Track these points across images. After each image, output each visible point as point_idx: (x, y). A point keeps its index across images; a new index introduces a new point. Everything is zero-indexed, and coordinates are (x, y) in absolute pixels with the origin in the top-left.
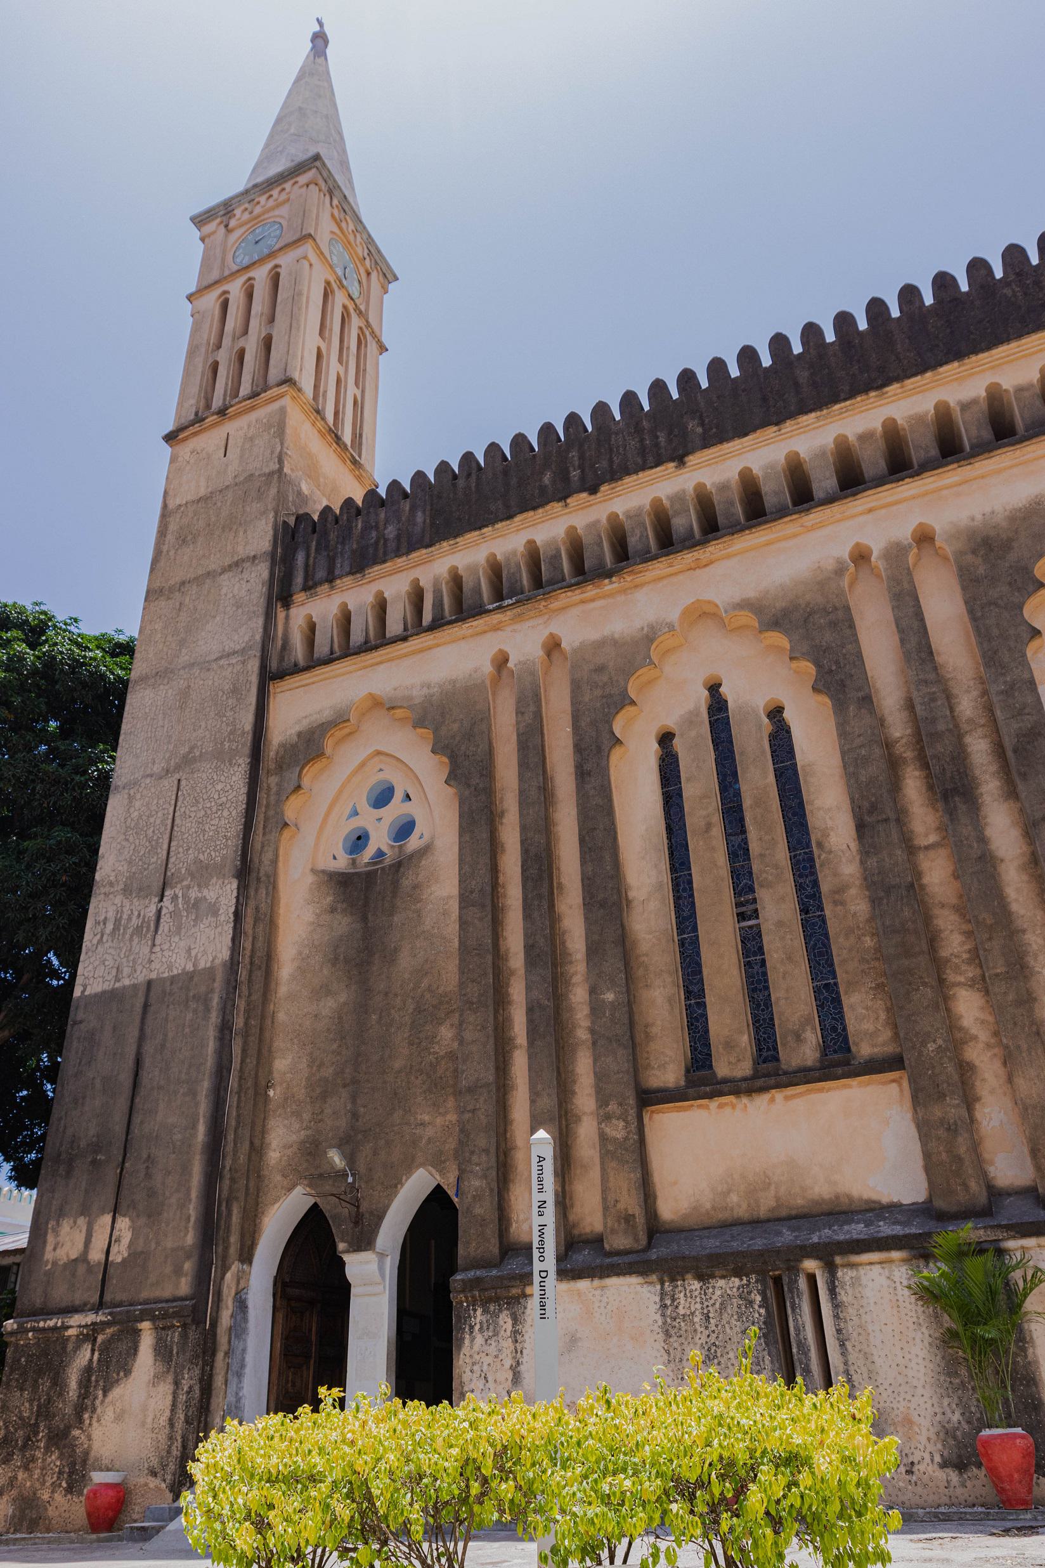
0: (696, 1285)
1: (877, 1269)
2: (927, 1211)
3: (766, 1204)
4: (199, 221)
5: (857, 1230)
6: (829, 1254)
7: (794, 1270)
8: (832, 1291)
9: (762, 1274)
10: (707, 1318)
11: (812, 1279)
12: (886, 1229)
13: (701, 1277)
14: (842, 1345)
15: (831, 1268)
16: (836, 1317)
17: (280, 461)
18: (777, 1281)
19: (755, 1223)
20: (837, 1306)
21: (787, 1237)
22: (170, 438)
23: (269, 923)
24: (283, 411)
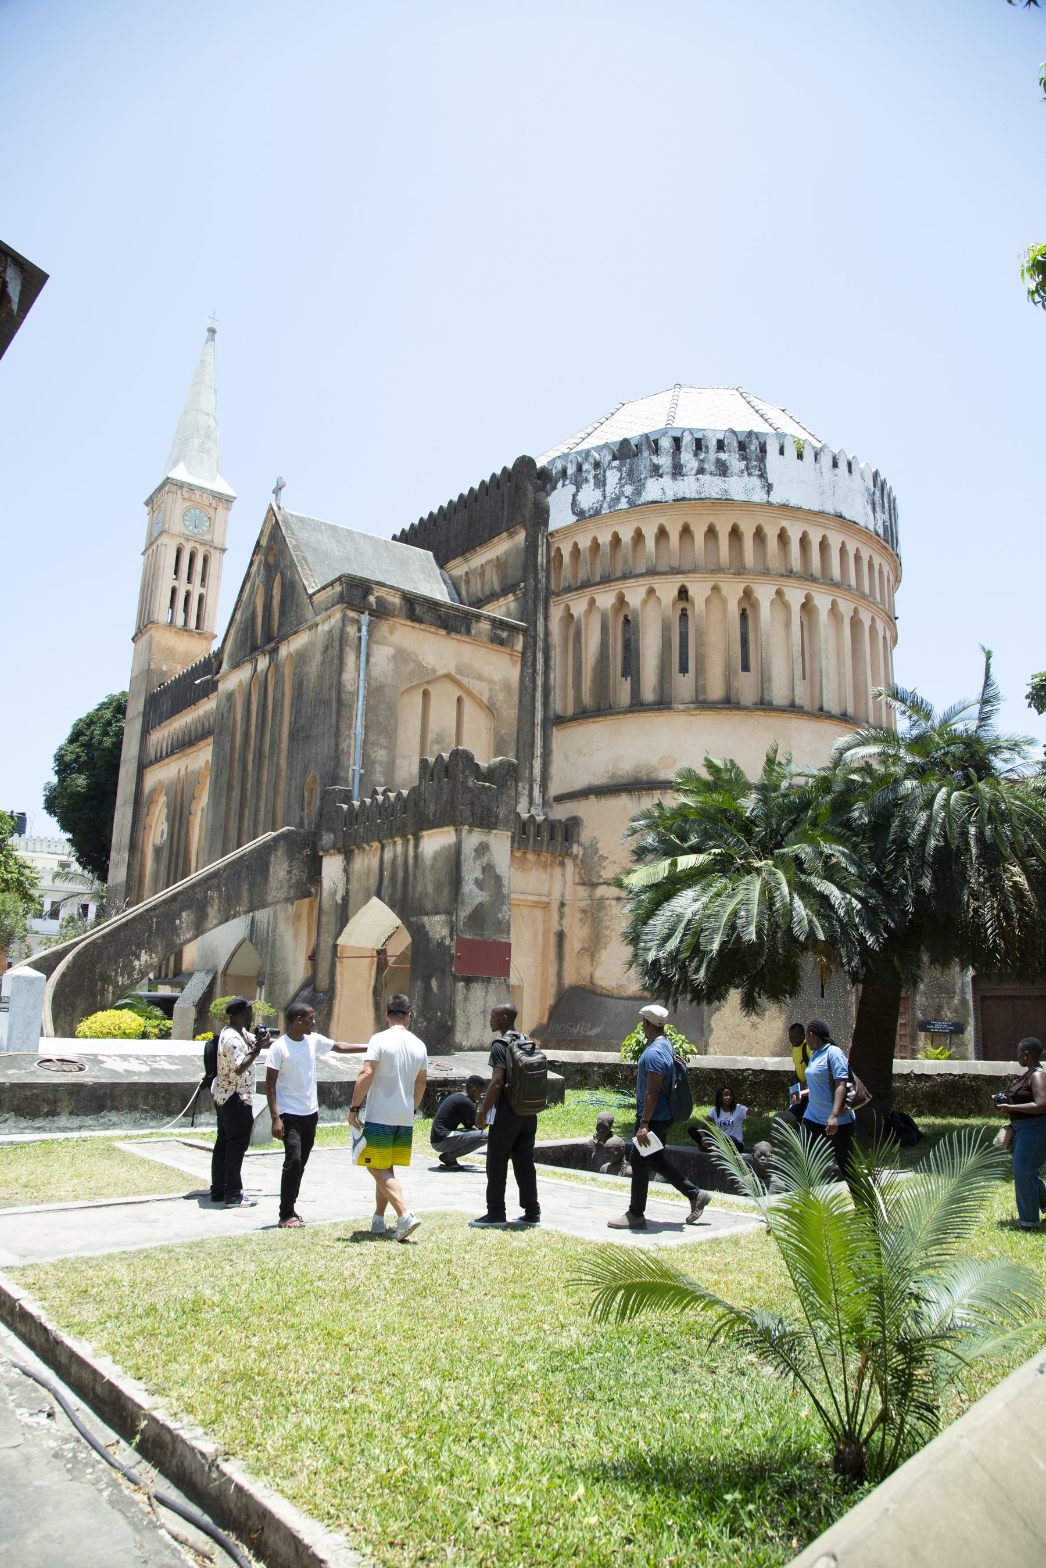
4: (147, 503)
17: (149, 665)
22: (133, 639)
23: (142, 865)
24: (151, 637)
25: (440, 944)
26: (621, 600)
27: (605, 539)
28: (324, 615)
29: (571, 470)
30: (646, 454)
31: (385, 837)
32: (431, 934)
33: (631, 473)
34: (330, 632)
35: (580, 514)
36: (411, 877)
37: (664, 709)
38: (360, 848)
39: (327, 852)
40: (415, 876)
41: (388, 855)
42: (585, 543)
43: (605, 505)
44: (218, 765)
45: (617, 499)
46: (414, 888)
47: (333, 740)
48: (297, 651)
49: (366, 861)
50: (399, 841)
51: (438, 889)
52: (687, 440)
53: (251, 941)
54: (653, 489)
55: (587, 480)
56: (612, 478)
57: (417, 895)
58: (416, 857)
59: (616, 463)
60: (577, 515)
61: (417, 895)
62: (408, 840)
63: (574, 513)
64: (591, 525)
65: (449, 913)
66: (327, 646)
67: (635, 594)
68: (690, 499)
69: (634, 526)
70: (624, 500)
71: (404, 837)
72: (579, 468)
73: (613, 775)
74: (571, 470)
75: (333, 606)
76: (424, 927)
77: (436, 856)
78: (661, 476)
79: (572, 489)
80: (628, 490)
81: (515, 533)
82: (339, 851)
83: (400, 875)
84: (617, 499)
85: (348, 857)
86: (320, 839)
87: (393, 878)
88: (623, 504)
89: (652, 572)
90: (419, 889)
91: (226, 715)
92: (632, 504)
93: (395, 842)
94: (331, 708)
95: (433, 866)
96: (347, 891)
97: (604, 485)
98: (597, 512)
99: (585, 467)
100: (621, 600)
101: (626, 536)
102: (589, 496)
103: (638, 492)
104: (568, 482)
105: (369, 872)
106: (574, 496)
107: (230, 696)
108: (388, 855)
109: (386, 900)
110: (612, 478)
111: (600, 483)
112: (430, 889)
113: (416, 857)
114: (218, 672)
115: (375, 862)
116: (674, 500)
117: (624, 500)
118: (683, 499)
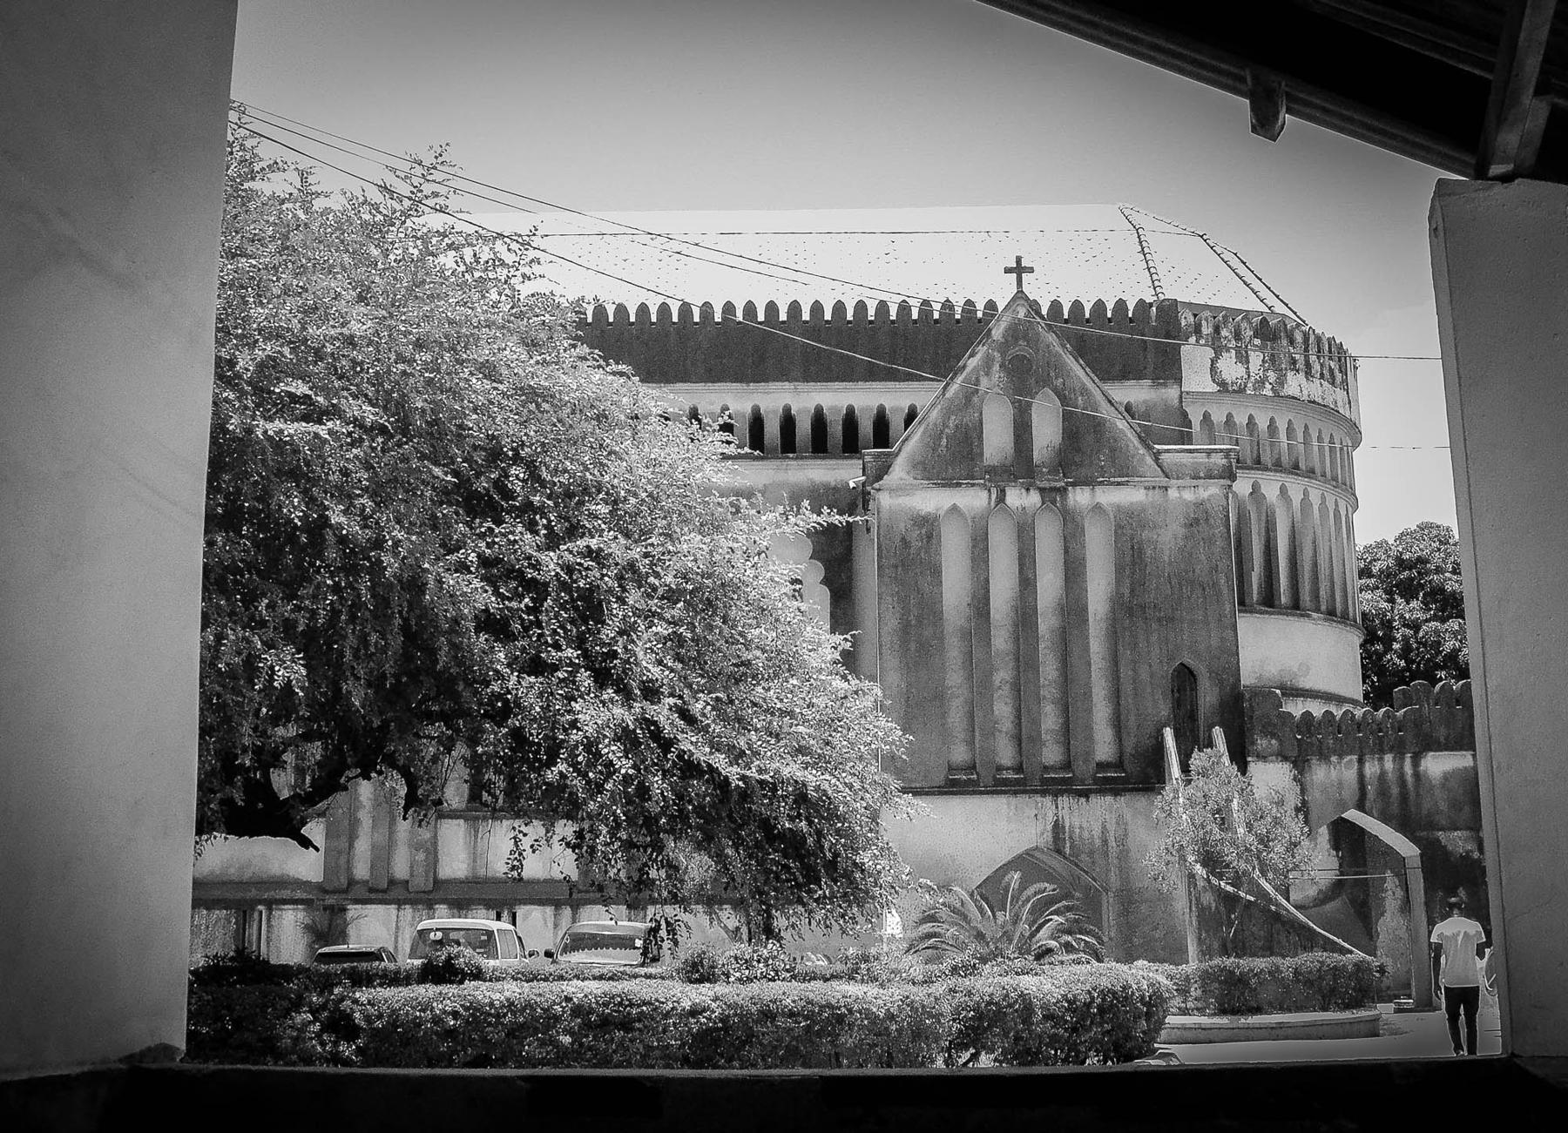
0: (205, 912)
1: (291, 912)
2: (321, 888)
3: (247, 875)
5: (286, 894)
6: (271, 904)
7: (253, 909)
8: (269, 920)
9: (238, 909)
10: (208, 927)
11: (261, 912)
12: (299, 895)
13: (207, 909)
14: (268, 943)
15: (270, 910)
16: (268, 931)
18: (245, 912)
19: (241, 884)
20: (269, 926)
21: (253, 893)
25: (1466, 857)
26: (1256, 488)
27: (1241, 419)
28: (1188, 482)
29: (1207, 330)
30: (1285, 342)
31: (1372, 753)
32: (1450, 848)
33: (1273, 358)
34: (1199, 504)
35: (1223, 384)
36: (1412, 795)
37: (1302, 616)
38: (1324, 757)
39: (1262, 757)
40: (1418, 795)
41: (1371, 769)
42: (1218, 417)
43: (1250, 385)
44: (906, 611)
45: (1261, 382)
46: (1419, 806)
47: (1230, 633)
48: (1119, 509)
49: (1334, 774)
50: (1388, 758)
51: (1455, 805)
52: (1312, 338)
53: (1059, 851)
54: (1295, 384)
55: (1228, 350)
56: (1256, 359)
57: (1424, 812)
58: (1417, 775)
59: (1257, 342)
60: (1218, 384)
61: (1424, 812)
62: (1402, 759)
63: (1214, 381)
64: (1227, 399)
65: (1470, 829)
66: (1197, 521)
67: (1271, 489)
68: (1319, 404)
69: (1270, 414)
70: (1268, 386)
71: (1399, 753)
72: (1217, 329)
73: (1260, 678)
74: (1207, 330)
75: (1211, 477)
76: (1438, 841)
77: (1447, 777)
78: (1297, 371)
79: (1210, 353)
80: (1272, 376)
81: (1165, 385)
82: (1285, 759)
83: (1395, 791)
84: (1261, 382)
85: (1300, 764)
86: (1253, 743)
87: (1383, 791)
88: (1268, 391)
89: (1278, 466)
90: (1426, 805)
91: (916, 544)
92: (1277, 395)
93: (1381, 759)
94: (1219, 594)
95: (1443, 786)
96: (1304, 802)
97: (1248, 362)
98: (1241, 390)
99: (1224, 333)
100: (1256, 488)
101: (1262, 423)
102: (1230, 369)
103: (1281, 381)
104: (1202, 342)
105: (1340, 783)
106: (1212, 361)
107: (928, 526)
108: (1371, 769)
109: (1375, 815)
110: (1256, 359)
111: (1243, 358)
112: (1443, 806)
113: (1417, 775)
114: (881, 479)
115: (1350, 775)
116: (1310, 402)
117: (1268, 386)
118: (1314, 402)
